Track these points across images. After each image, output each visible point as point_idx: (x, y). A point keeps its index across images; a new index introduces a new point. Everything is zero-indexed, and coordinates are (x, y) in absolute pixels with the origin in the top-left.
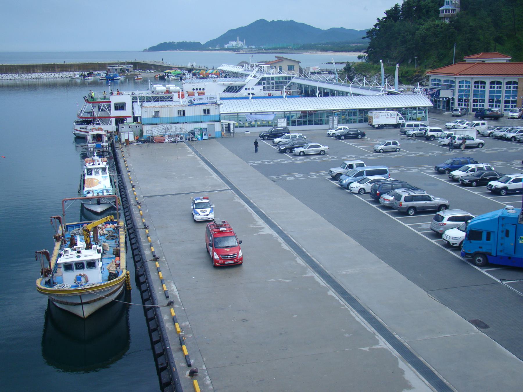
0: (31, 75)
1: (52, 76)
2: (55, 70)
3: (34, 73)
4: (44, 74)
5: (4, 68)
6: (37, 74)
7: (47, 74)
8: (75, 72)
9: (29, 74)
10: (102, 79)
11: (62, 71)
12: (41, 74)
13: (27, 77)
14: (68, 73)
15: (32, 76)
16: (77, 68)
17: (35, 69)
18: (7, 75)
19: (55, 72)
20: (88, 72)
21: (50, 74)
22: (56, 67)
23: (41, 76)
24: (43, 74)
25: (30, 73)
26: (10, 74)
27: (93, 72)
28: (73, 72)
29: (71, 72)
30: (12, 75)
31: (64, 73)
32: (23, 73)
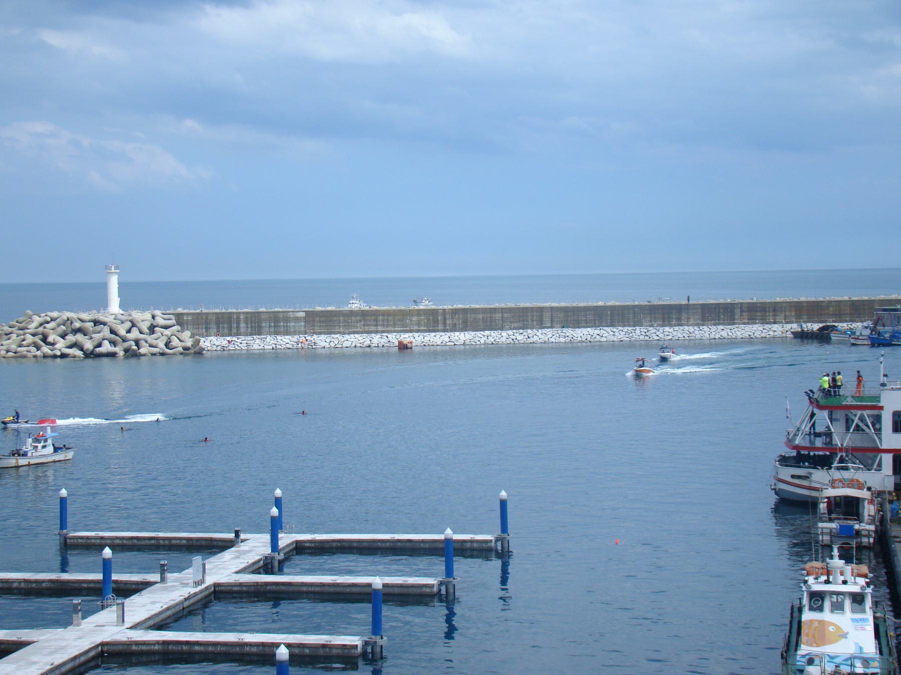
0: (671, 330)
1: (724, 334)
2: (734, 319)
3: (679, 325)
4: (705, 328)
5: (609, 313)
6: (686, 328)
7: (713, 328)
8: (787, 323)
9: (667, 329)
10: (859, 342)
11: (752, 320)
12: (696, 328)
13: (661, 336)
14: (767, 326)
15: (675, 333)
16: (793, 314)
17: (684, 316)
18: (615, 330)
19: (734, 324)
20: (821, 325)
21: (721, 327)
22: (737, 311)
23: (697, 332)
24: (701, 328)
25: (671, 326)
26: (620, 328)
27: (836, 324)
28: (779, 323)
29: (775, 323)
30: (625, 329)
31: (757, 326)
32: (651, 326)
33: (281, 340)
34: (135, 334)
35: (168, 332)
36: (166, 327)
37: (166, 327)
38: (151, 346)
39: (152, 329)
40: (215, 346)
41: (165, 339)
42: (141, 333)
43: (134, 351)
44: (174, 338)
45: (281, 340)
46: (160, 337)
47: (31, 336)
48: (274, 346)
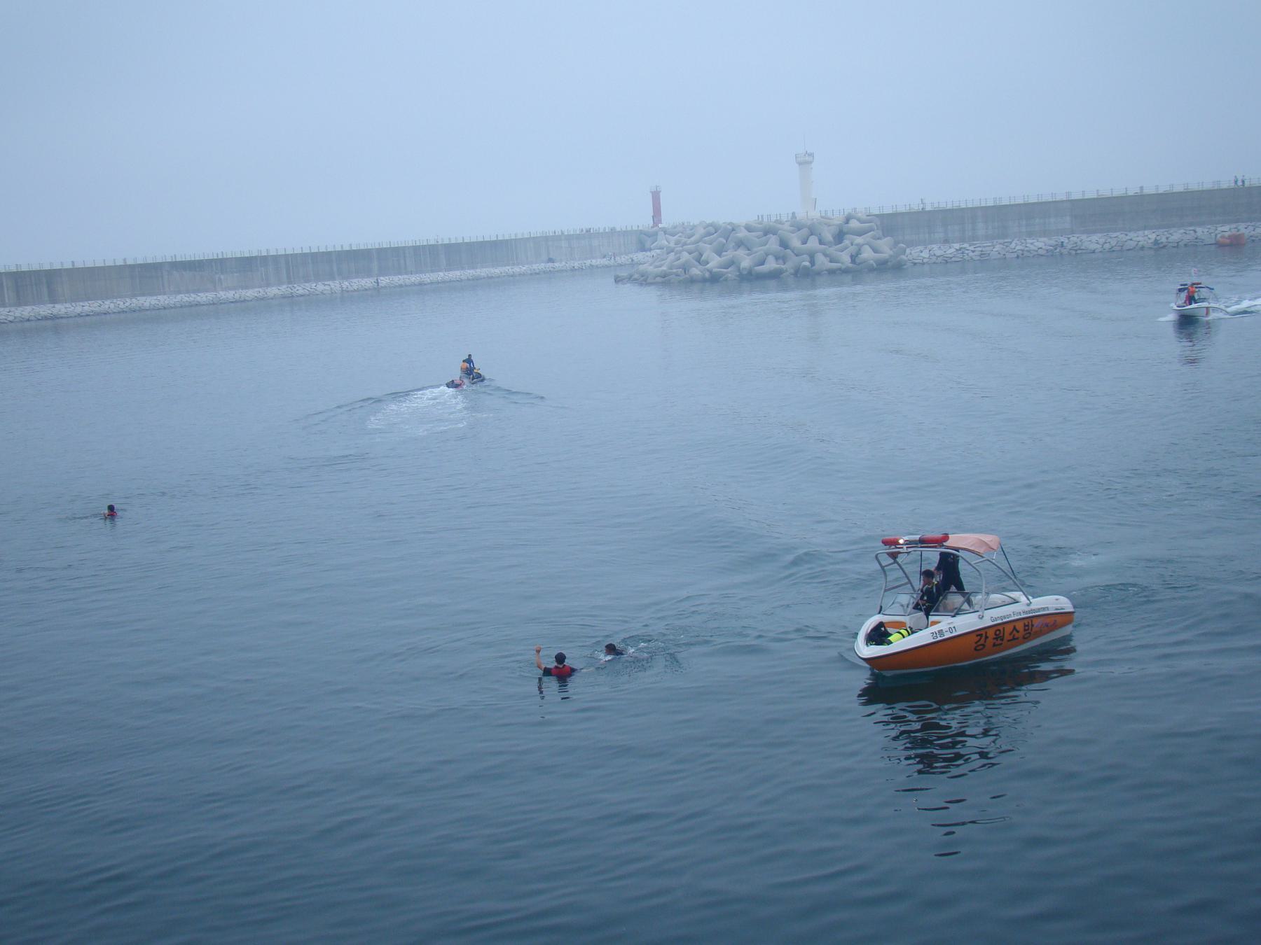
33: (1032, 244)
34: (813, 243)
35: (859, 240)
36: (860, 233)
37: (860, 233)
38: (831, 262)
39: (840, 236)
40: (934, 258)
41: (852, 249)
42: (821, 242)
43: (805, 267)
44: (867, 248)
45: (1032, 244)
46: (847, 248)
47: (687, 254)
48: (1021, 252)
